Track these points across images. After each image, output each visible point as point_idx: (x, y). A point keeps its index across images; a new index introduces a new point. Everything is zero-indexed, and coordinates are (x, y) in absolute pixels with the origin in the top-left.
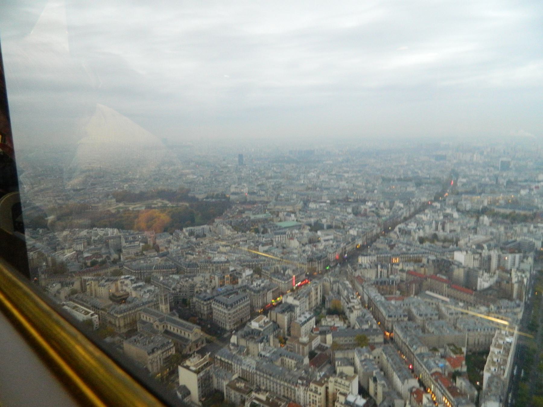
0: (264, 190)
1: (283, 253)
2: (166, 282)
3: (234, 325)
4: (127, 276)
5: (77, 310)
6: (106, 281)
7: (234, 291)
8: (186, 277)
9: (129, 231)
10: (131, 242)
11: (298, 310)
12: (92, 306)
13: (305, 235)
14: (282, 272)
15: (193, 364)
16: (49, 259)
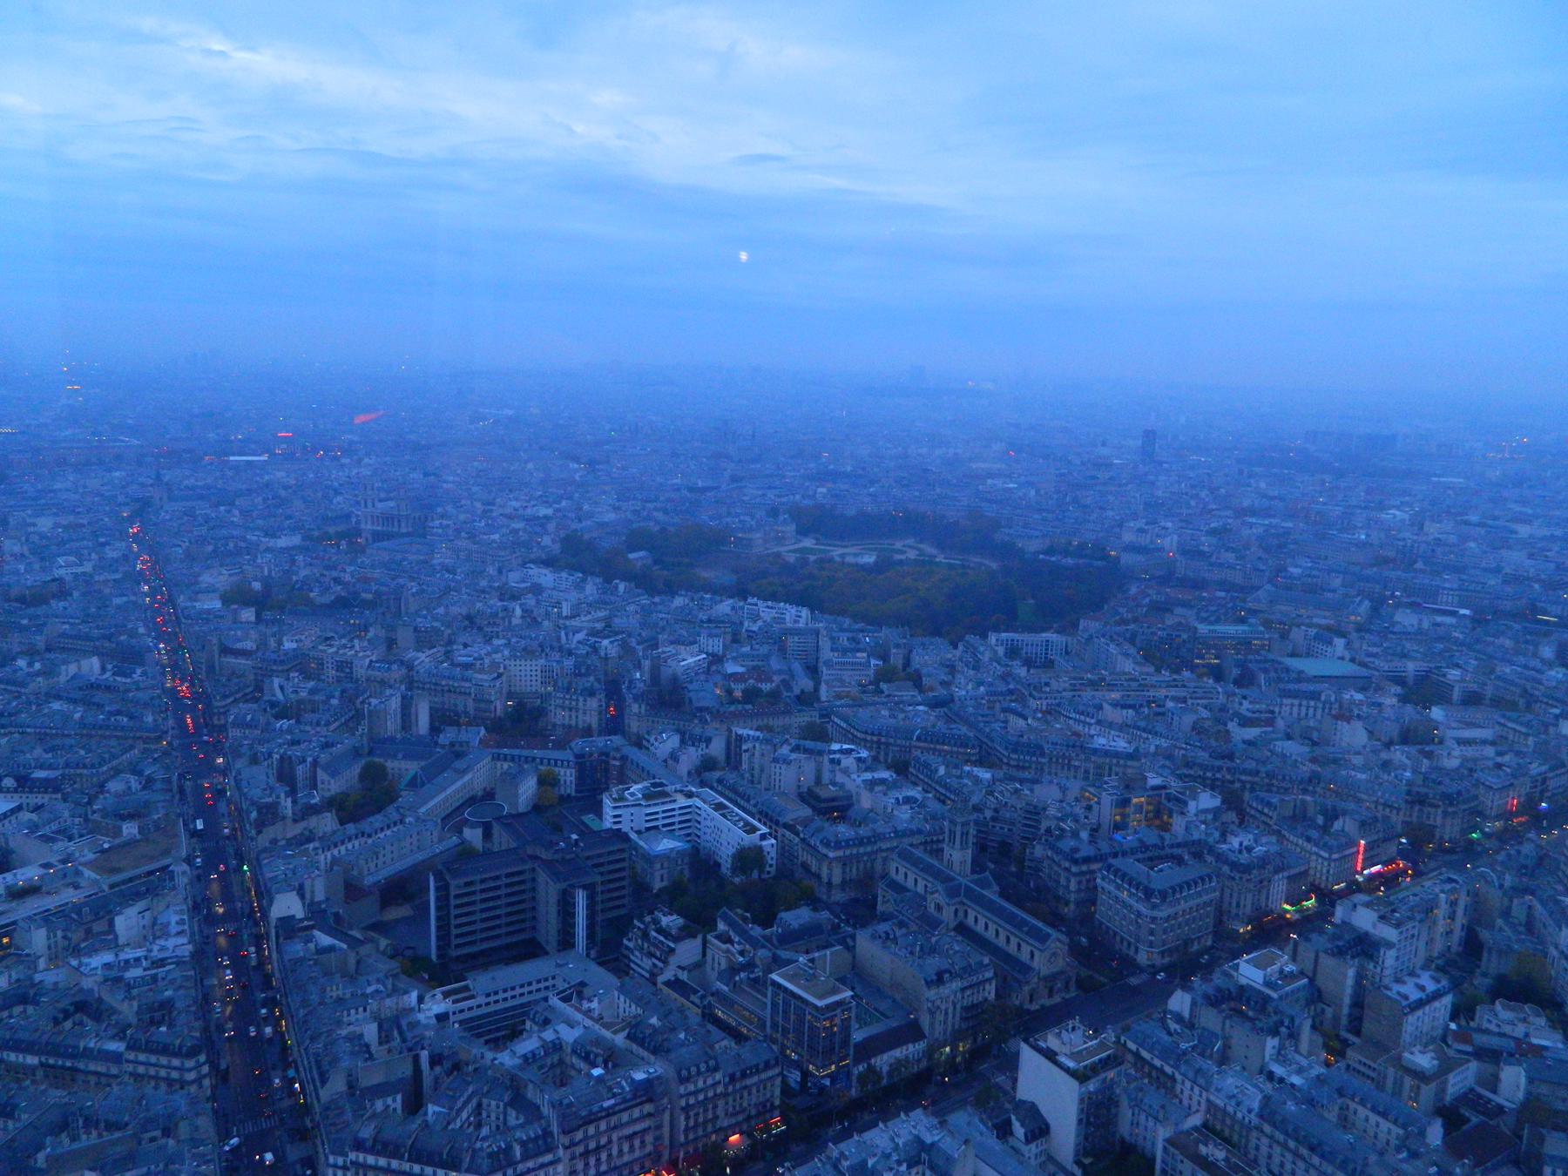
0: (1233, 550)
1: (1314, 760)
2: (954, 783)
3: (1162, 954)
4: (846, 746)
5: (724, 816)
7: (1168, 851)
8: (1013, 779)
10: (845, 651)
11: (1389, 958)
12: (761, 813)
13: (1388, 713)
14: (1320, 820)
16: (647, 664)
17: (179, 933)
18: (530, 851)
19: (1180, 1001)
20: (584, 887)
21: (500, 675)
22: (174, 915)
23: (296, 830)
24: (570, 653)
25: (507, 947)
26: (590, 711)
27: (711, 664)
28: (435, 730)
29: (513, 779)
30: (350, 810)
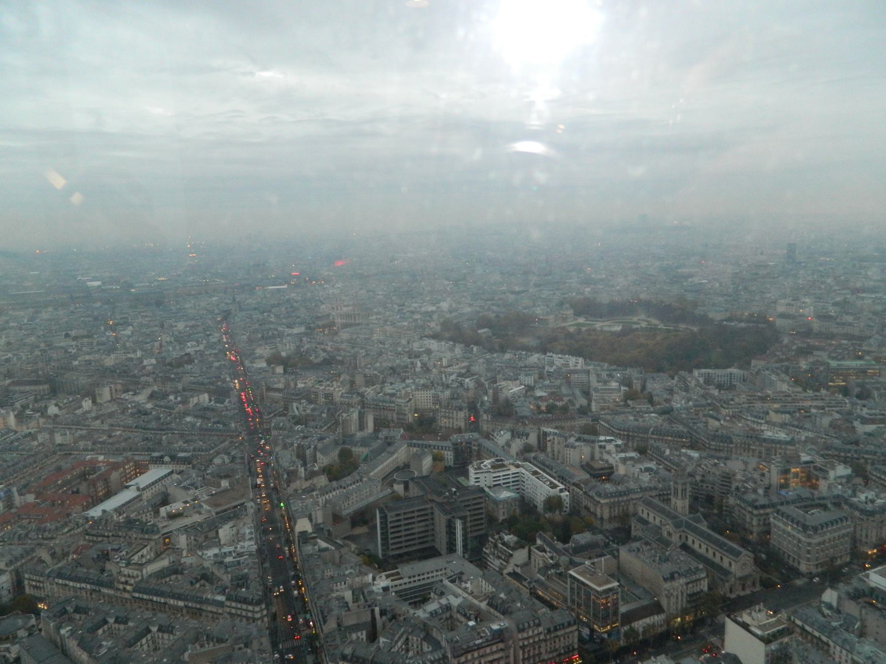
0: (851, 314)
2: (676, 459)
3: (817, 566)
4: (608, 438)
5: (538, 478)
6: (577, 440)
7: (817, 502)
8: (712, 457)
15: (755, 623)
17: (250, 539)
18: (429, 497)
19: (830, 596)
20: (460, 518)
21: (410, 400)
22: (247, 530)
23: (306, 485)
24: (448, 387)
25: (419, 551)
26: (460, 418)
27: (527, 391)
28: (377, 430)
29: (419, 457)
30: (334, 474)
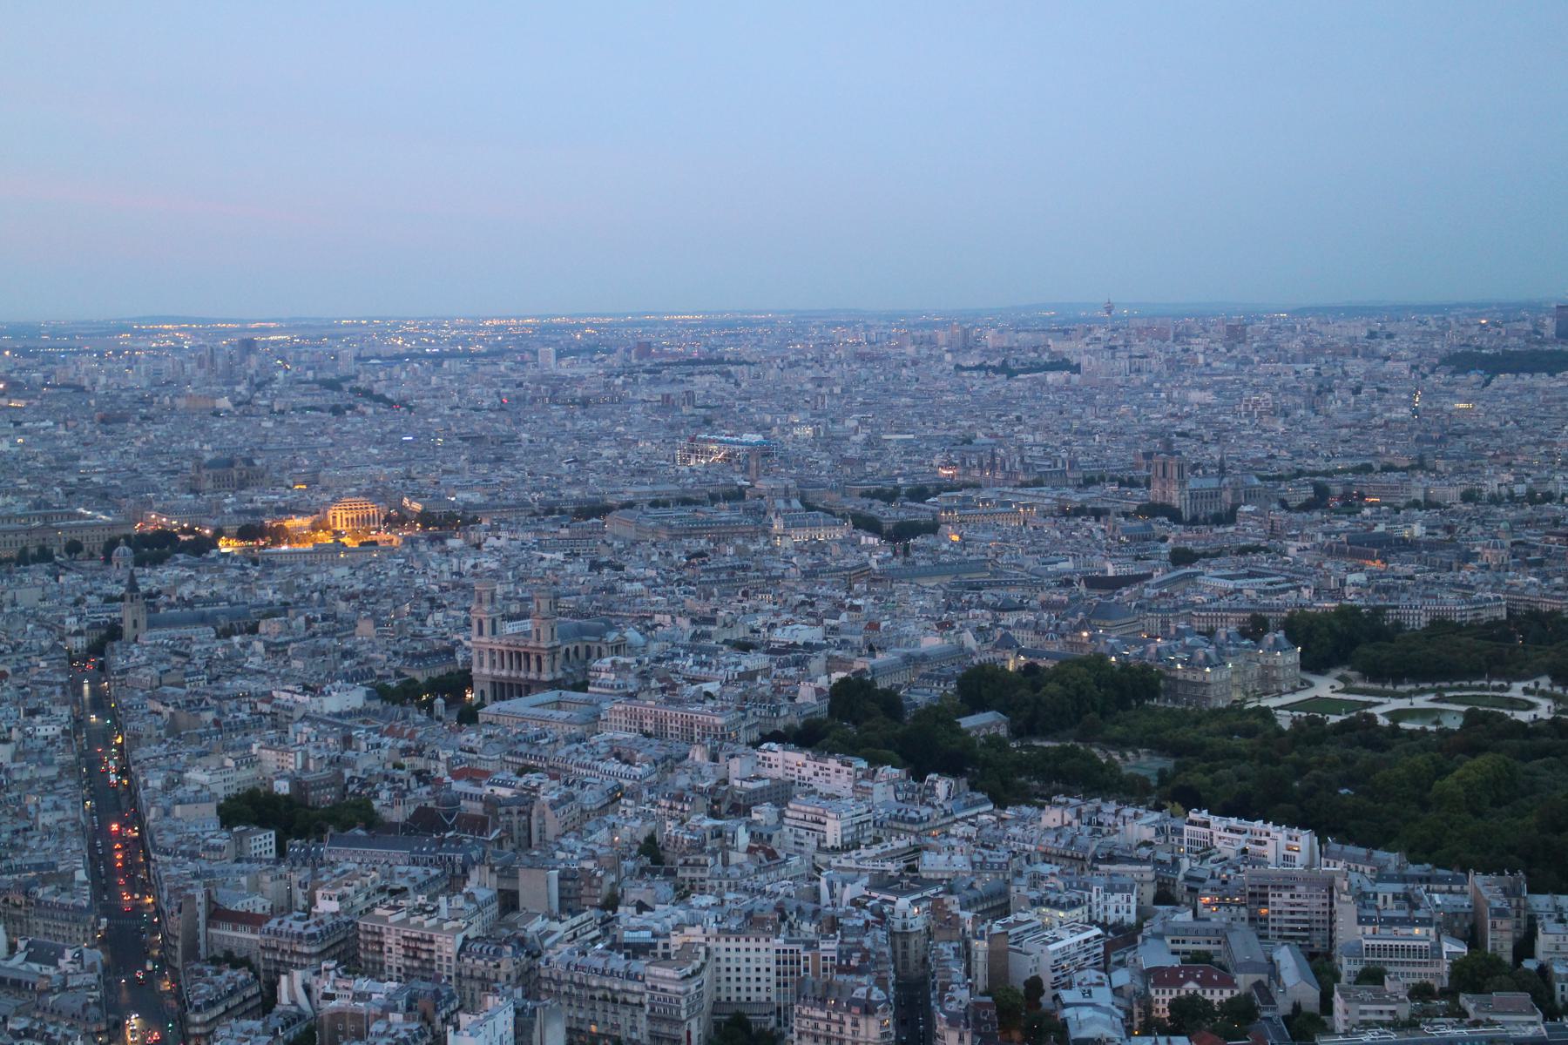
9: (1379, 854)
27: (1109, 948)
